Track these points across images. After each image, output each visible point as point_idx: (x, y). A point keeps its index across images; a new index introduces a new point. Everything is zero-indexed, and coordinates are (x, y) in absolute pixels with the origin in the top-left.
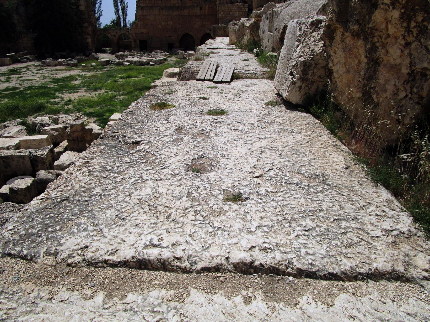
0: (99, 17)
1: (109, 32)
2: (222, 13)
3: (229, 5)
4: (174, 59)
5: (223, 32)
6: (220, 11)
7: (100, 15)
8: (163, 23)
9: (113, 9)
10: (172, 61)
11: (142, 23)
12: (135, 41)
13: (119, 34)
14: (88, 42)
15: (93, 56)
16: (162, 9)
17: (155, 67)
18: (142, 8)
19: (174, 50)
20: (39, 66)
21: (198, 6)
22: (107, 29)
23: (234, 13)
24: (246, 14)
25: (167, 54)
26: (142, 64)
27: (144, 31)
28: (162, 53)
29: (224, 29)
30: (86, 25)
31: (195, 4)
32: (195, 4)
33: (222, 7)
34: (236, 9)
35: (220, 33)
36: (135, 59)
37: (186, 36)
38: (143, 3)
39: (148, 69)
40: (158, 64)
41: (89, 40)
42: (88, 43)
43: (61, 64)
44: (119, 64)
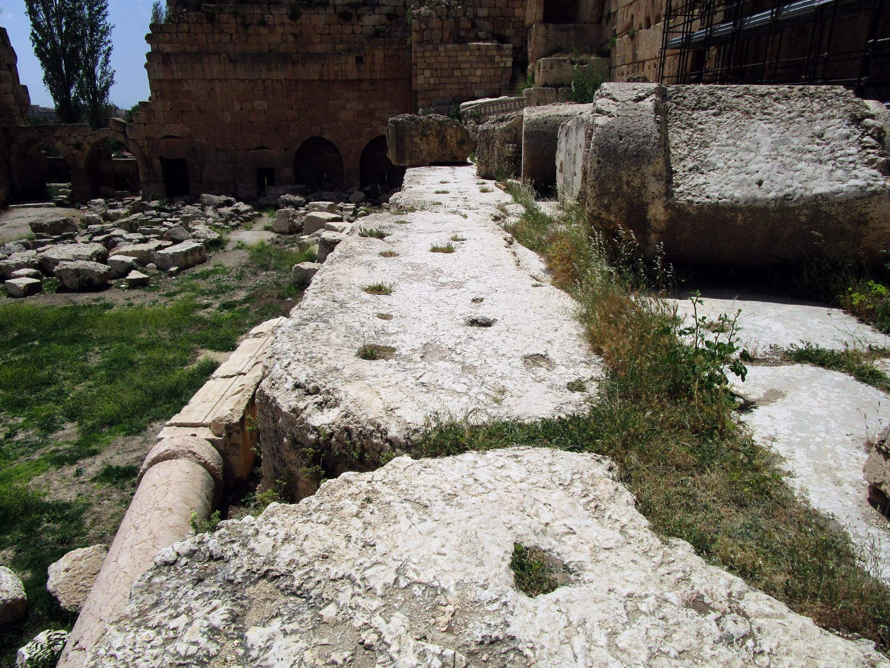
0: (106, 88)
1: (58, 134)
3: (450, 46)
4: (253, 236)
5: (434, 143)
7: (108, 84)
8: (237, 106)
10: (241, 246)
12: (149, 163)
13: (91, 139)
16: (233, 61)
17: (139, 297)
19: (272, 190)
23: (467, 72)
24: (508, 75)
25: (243, 207)
26: (89, 283)
27: (176, 129)
28: (229, 204)
29: (438, 133)
32: (340, 47)
33: (428, 54)
34: (474, 59)
35: (424, 147)
38: (169, 42)
40: (172, 274)
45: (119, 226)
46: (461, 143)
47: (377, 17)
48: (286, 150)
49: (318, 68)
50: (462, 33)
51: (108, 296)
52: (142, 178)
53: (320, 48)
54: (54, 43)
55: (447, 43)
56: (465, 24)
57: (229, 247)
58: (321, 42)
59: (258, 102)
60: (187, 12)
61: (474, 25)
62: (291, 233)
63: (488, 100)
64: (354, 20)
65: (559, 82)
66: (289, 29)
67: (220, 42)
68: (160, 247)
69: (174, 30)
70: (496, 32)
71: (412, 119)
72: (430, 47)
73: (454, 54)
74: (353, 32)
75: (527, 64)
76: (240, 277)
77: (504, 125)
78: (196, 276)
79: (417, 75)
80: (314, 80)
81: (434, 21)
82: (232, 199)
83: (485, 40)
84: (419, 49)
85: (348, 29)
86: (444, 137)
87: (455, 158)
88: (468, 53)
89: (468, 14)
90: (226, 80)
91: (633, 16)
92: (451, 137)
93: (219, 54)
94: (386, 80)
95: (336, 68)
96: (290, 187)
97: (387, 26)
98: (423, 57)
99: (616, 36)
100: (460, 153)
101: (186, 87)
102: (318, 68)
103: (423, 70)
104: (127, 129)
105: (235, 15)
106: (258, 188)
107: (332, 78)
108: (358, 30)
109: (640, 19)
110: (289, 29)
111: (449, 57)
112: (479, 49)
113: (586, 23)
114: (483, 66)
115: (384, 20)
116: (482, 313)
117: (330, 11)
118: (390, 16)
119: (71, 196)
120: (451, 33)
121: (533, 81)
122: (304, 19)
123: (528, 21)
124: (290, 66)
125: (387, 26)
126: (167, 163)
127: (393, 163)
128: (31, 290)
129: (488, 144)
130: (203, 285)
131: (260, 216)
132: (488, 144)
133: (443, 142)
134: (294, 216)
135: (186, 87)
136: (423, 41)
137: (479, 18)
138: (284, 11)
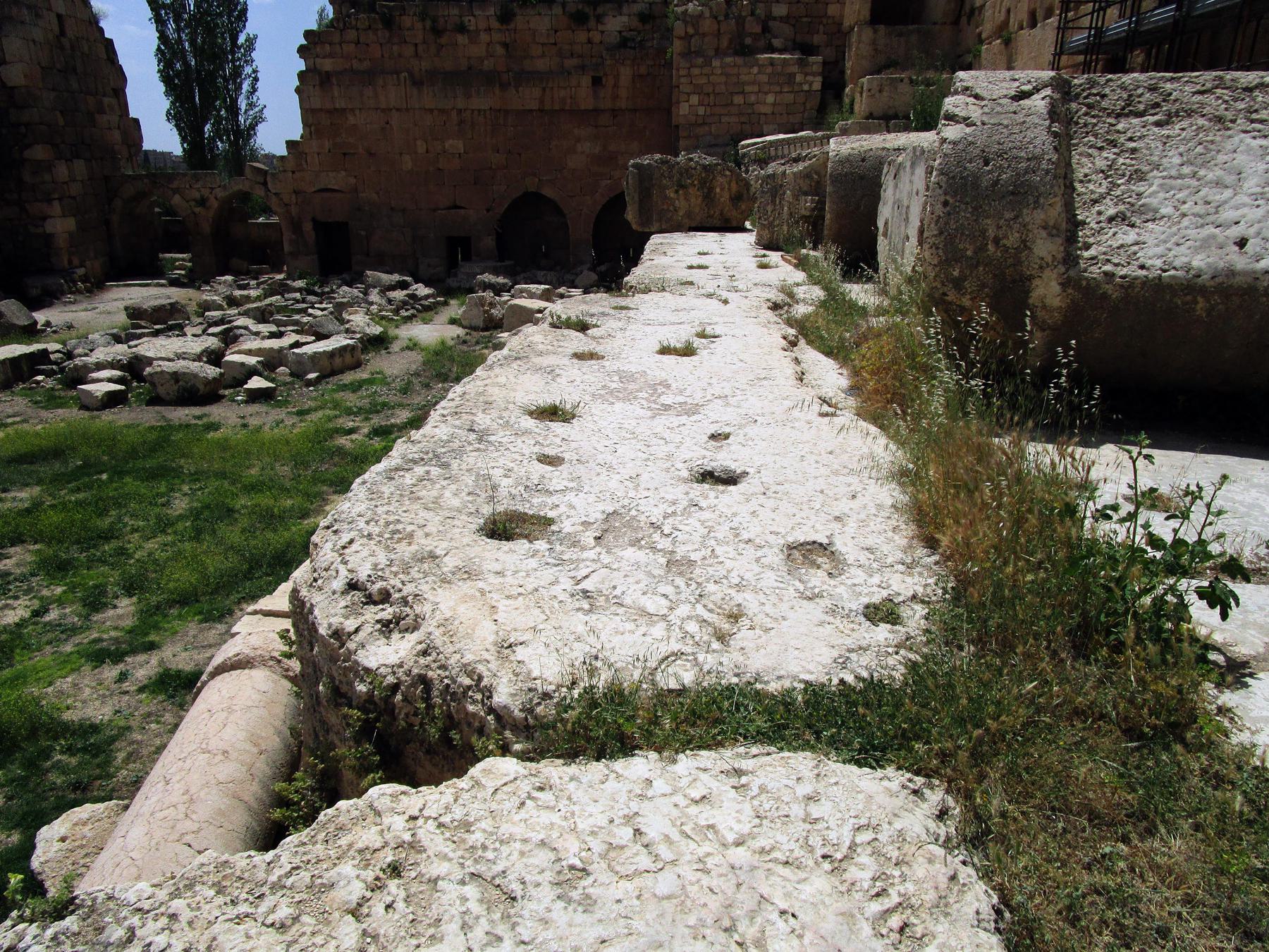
0: (253, 127)
1: (175, 185)
2: (695, 99)
3: (729, 60)
4: (430, 332)
6: (683, 88)
7: (258, 119)
8: (421, 147)
10: (413, 346)
11: (327, 145)
12: (296, 227)
13: (220, 193)
14: (51, 236)
16: (417, 83)
17: (260, 415)
19: (465, 268)
21: (583, 68)
23: (753, 98)
24: (814, 102)
25: (422, 290)
27: (336, 180)
28: (403, 285)
29: (703, 183)
30: (39, 152)
32: (570, 63)
33: (696, 71)
34: (765, 78)
35: (681, 204)
37: (530, 205)
38: (331, 56)
40: (309, 383)
42: (49, 238)
45: (246, 314)
46: (737, 199)
47: (625, 19)
48: (488, 210)
49: (537, 92)
50: (748, 41)
51: (216, 412)
52: (287, 248)
53: (541, 65)
54: (186, 64)
55: (726, 55)
56: (753, 27)
57: (395, 347)
58: (543, 55)
59: (451, 141)
60: (357, 12)
61: (766, 29)
62: (486, 329)
63: (781, 136)
64: (592, 23)
65: (891, 112)
66: (497, 37)
67: (400, 56)
68: (297, 344)
69: (337, 38)
70: (799, 39)
71: (663, 162)
72: (700, 60)
73: (735, 71)
74: (590, 41)
75: (844, 87)
76: (405, 391)
77: (801, 166)
78: (344, 388)
79: (678, 102)
81: (708, 22)
82: (408, 279)
83: (781, 51)
84: (683, 64)
85: (582, 36)
86: (711, 189)
87: (727, 220)
88: (755, 70)
89: (758, 11)
90: (407, 110)
91: (1009, 11)
92: (722, 189)
93: (398, 73)
94: (635, 110)
95: (563, 93)
96: (490, 264)
97: (639, 32)
98: (689, 75)
99: (981, 42)
100: (734, 213)
101: (352, 120)
102: (537, 92)
103: (689, 94)
104: (269, 179)
105: (423, 17)
107: (557, 107)
108: (597, 37)
109: (1022, 14)
110: (497, 37)
111: (727, 75)
112: (772, 64)
113: (935, 24)
114: (778, 89)
115: (635, 23)
116: (723, 459)
117: (557, 10)
118: (644, 18)
119: (191, 271)
120: (731, 41)
121: (852, 111)
122: (519, 22)
123: (847, 23)
124: (497, 92)
125: (639, 32)
127: (634, 227)
128: (112, 400)
129: (774, 197)
130: (351, 399)
131: (446, 304)
132: (774, 197)
133: (709, 197)
134: (492, 305)
135: (352, 120)
136: (690, 53)
137: (775, 19)
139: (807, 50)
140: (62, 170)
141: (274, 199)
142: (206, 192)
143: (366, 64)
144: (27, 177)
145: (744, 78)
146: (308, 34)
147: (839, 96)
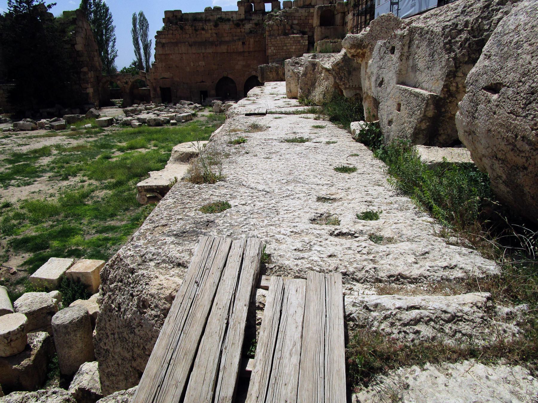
0: (113, 59)
2: (272, 48)
3: (282, 37)
4: (207, 113)
5: (274, 74)
6: (270, 45)
7: (115, 56)
8: (192, 64)
9: (133, 48)
10: (203, 116)
12: (155, 89)
13: (132, 80)
15: (92, 112)
16: (191, 45)
17: (177, 127)
18: (163, 45)
19: (208, 99)
20: (9, 130)
22: (126, 72)
23: (289, 47)
24: (307, 47)
25: (198, 105)
26: (158, 123)
27: (167, 75)
28: (192, 104)
29: (276, 70)
30: (85, 69)
31: (235, 38)
32: (235, 38)
33: (273, 40)
35: (271, 76)
36: (151, 116)
39: (166, 132)
40: (183, 122)
41: (90, 90)
42: (88, 94)
43: (42, 127)
44: (127, 124)
45: (155, 110)
47: (251, 25)
49: (226, 47)
50: (287, 31)
52: (152, 96)
53: (227, 39)
55: (281, 35)
56: (288, 27)
57: (199, 116)
61: (292, 27)
62: (220, 112)
64: (241, 26)
66: (214, 31)
80: (224, 53)
83: (296, 34)
84: (269, 38)
85: (239, 30)
86: (278, 72)
93: (185, 43)
94: (255, 51)
101: (171, 57)
102: (226, 47)
105: (192, 26)
106: (203, 98)
108: (243, 30)
110: (214, 31)
115: (254, 26)
117: (231, 23)
118: (256, 24)
122: (220, 26)
123: (314, 25)
126: (162, 89)
133: (277, 74)
135: (171, 57)
138: (212, 24)
139: (304, 33)
140: (90, 74)
141: (148, 81)
142: (127, 80)
143: (175, 40)
144: (82, 77)
145: (286, 42)
146: (158, 32)
147: (313, 46)
